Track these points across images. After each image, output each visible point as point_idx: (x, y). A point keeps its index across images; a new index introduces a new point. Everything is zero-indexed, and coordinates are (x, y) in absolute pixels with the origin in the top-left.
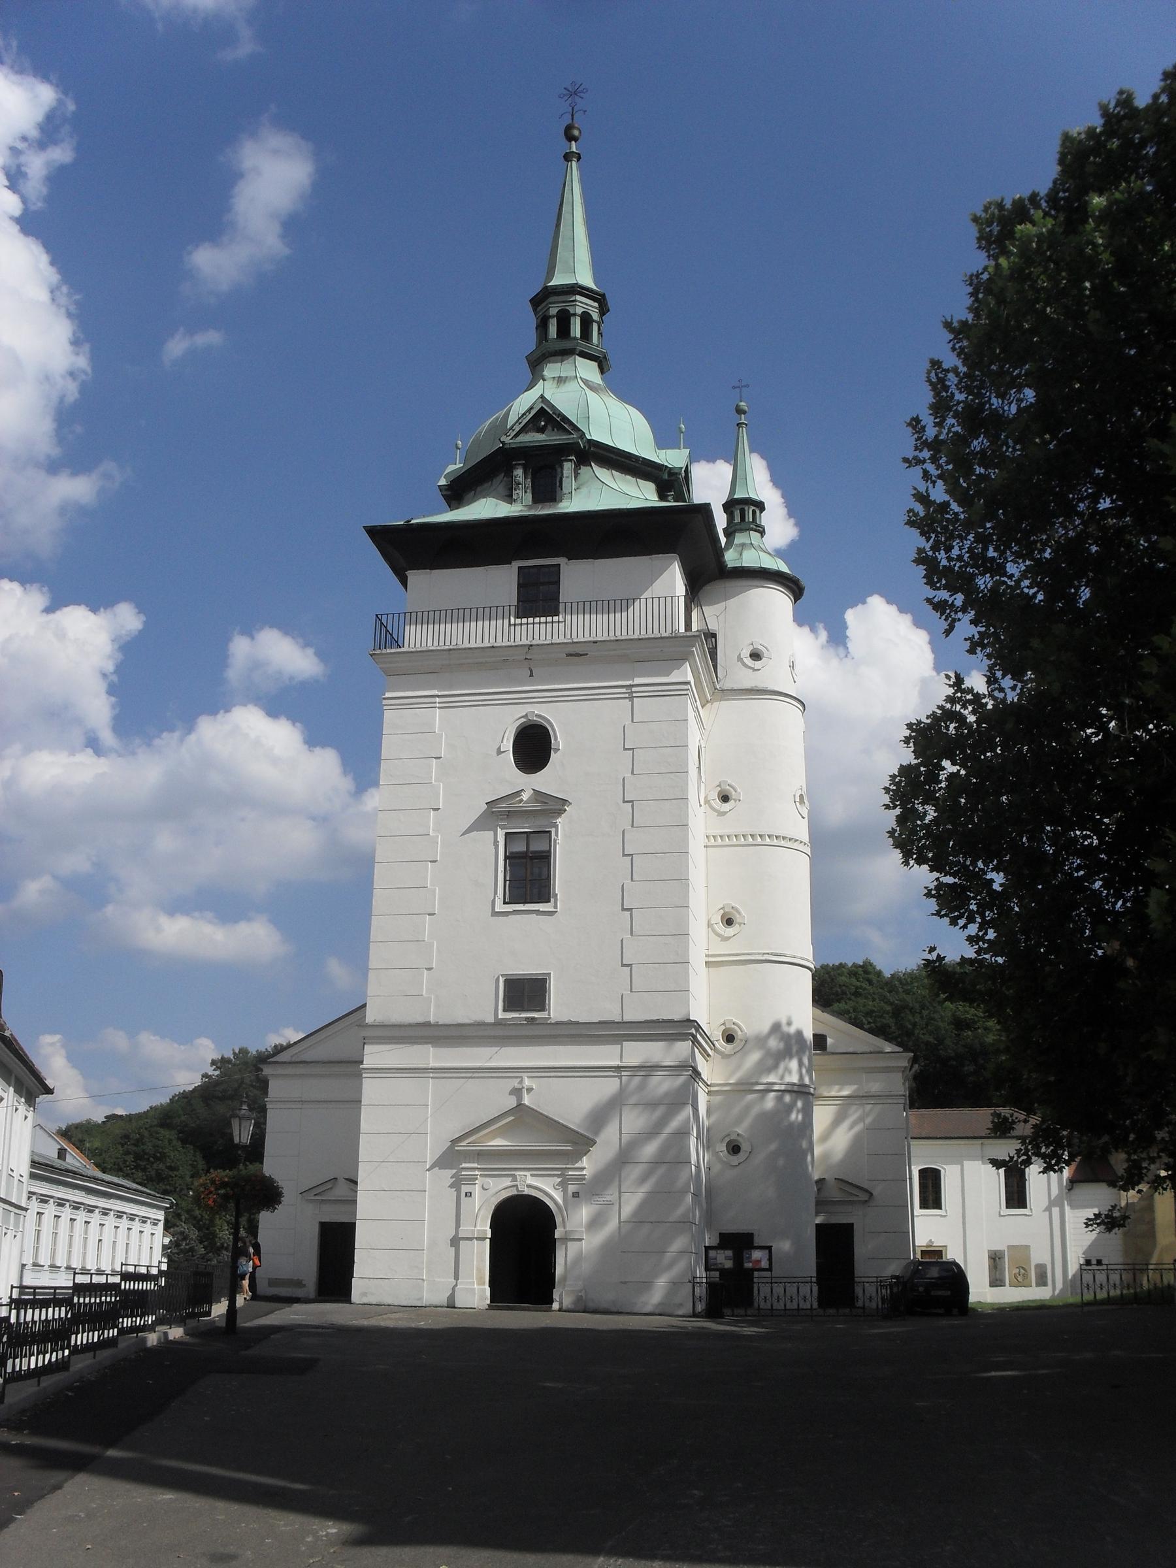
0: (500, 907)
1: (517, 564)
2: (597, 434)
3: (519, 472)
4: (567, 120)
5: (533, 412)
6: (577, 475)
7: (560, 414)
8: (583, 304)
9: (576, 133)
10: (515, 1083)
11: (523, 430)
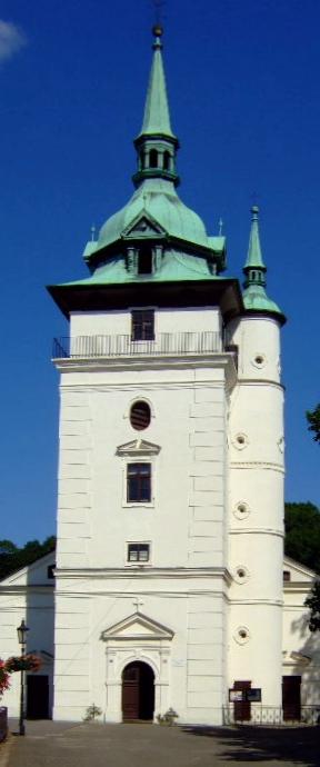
0: (125, 504)
1: (131, 309)
2: (174, 232)
6: (163, 256)
7: (154, 221)
8: (163, 146)
9: (159, 32)
10: (135, 601)
11: (133, 229)
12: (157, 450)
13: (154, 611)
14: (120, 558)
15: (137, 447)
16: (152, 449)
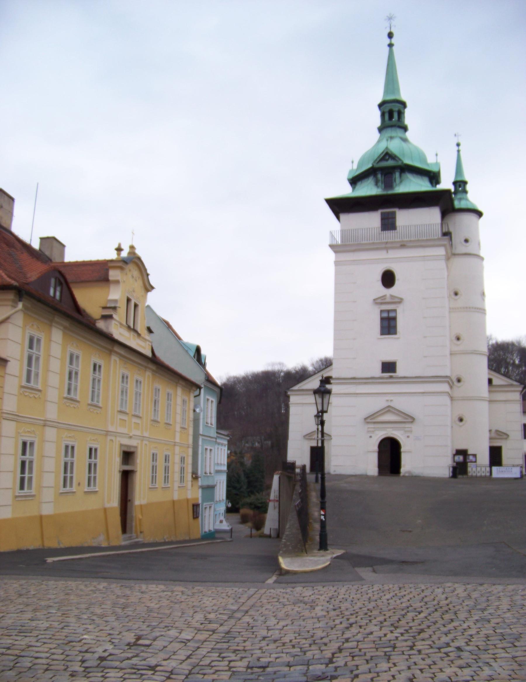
3: (379, 176)
4: (388, 31)
5: (384, 154)
12: (400, 301)
13: (400, 403)
14: (377, 371)
15: (388, 300)
16: (396, 300)
